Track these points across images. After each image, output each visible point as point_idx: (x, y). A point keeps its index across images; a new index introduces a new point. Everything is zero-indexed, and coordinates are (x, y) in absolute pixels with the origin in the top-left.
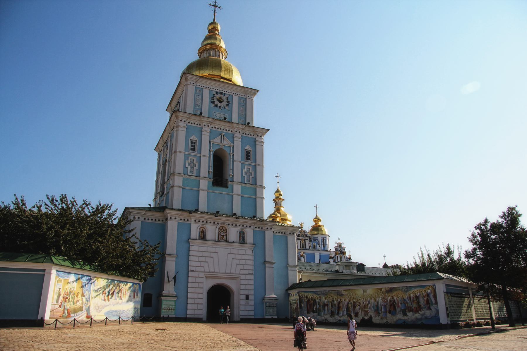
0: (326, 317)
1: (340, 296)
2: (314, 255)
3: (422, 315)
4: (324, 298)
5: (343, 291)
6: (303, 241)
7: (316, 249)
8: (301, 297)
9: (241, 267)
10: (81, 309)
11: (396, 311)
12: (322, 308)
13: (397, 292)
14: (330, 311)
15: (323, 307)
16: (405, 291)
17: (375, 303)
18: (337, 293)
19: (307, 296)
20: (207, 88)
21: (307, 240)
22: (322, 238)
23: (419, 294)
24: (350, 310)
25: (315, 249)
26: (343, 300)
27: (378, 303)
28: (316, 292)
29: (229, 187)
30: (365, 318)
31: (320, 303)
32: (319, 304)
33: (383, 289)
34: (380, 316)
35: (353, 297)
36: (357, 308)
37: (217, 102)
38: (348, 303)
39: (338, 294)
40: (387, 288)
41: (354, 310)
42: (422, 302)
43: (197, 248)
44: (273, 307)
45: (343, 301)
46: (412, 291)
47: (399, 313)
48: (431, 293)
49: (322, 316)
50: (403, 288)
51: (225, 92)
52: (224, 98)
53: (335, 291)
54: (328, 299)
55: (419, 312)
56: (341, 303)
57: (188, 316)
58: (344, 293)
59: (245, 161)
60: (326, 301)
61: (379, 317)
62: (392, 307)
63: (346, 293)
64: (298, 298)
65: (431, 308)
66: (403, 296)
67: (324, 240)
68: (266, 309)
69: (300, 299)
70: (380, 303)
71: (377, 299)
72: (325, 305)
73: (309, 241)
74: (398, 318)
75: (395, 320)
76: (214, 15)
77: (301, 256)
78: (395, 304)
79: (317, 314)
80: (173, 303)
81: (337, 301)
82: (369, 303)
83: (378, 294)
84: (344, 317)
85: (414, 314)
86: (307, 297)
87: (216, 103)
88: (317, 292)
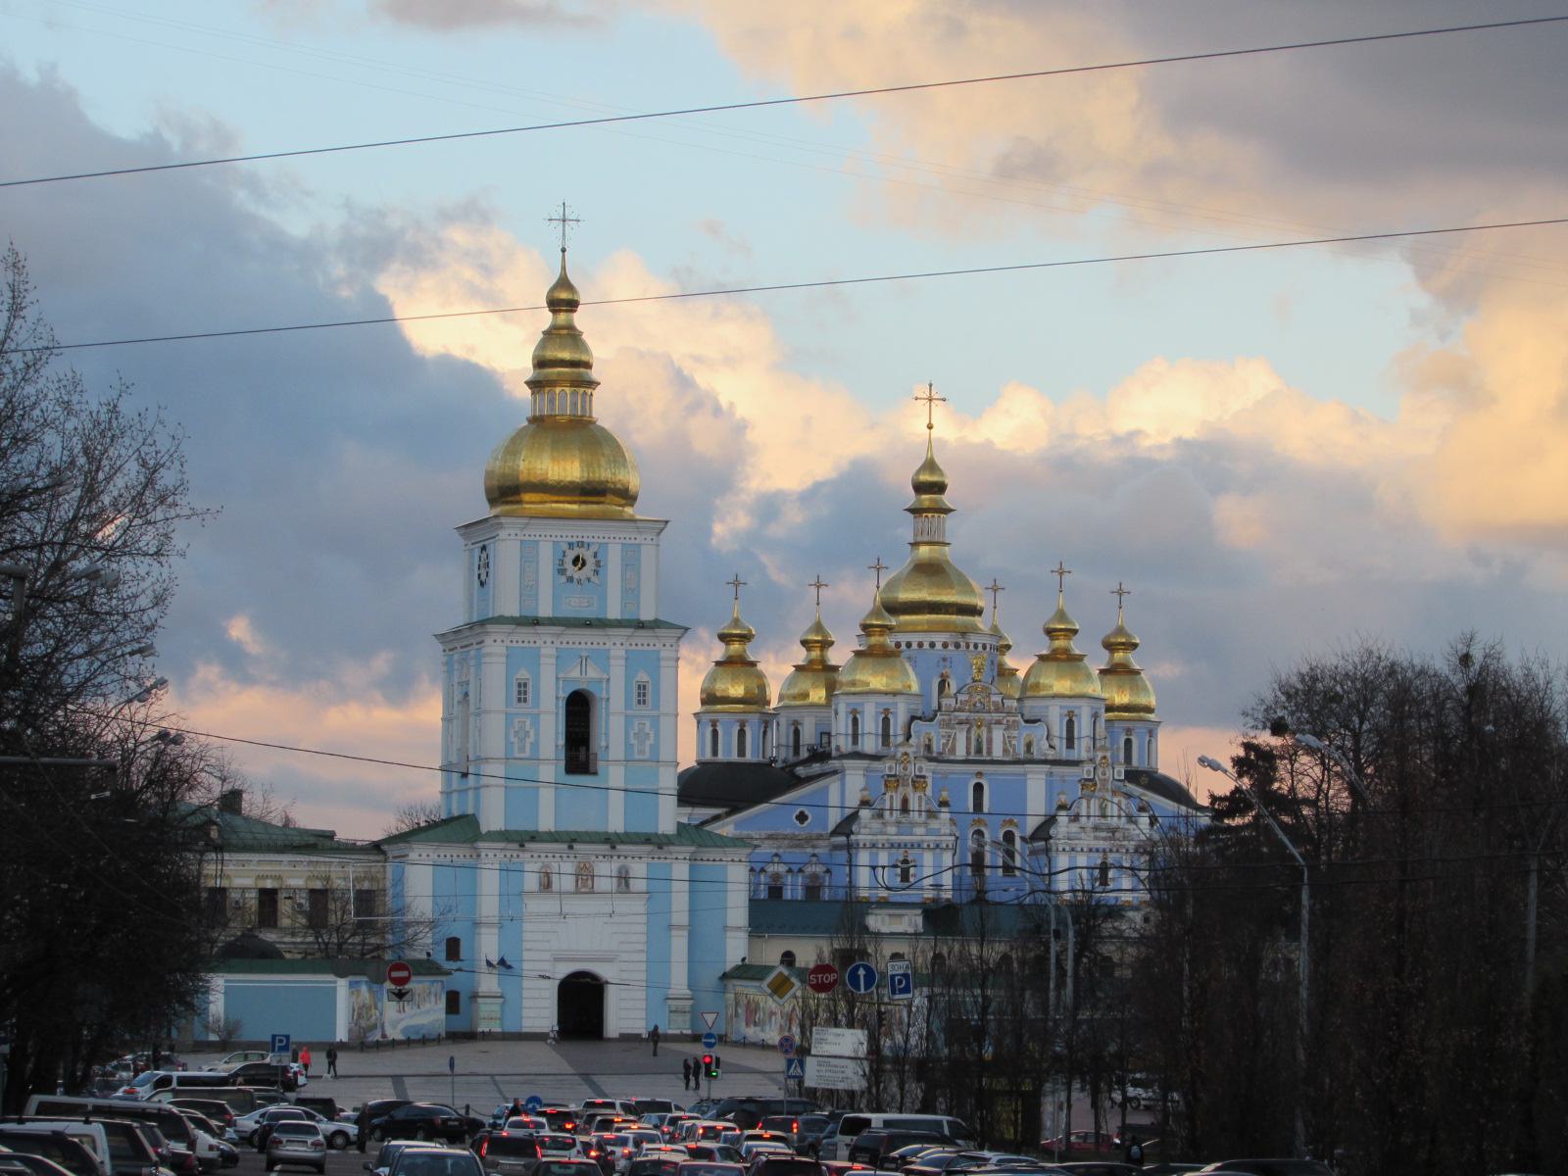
2: (1025, 780)
7: (1036, 756)
10: (375, 1027)
14: (778, 1026)
20: (548, 538)
21: (999, 722)
22: (1065, 712)
25: (1029, 756)
29: (599, 772)
37: (571, 569)
43: (535, 906)
44: (684, 1012)
51: (590, 540)
52: (587, 555)
57: (524, 1030)
59: (632, 709)
67: (1074, 718)
68: (669, 1016)
72: (772, 1013)
73: (1003, 727)
76: (564, 250)
77: (944, 804)
80: (497, 1008)
87: (569, 574)
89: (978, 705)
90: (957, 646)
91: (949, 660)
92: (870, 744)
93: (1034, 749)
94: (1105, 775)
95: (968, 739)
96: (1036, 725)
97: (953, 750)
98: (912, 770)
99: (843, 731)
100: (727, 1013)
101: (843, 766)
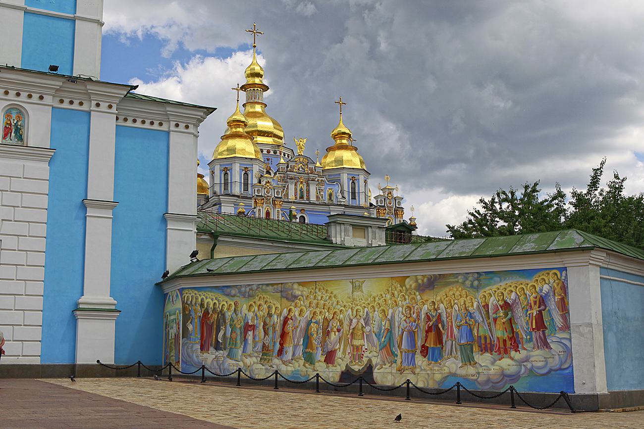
0: (249, 364)
1: (287, 299)
3: (520, 363)
4: (245, 306)
5: (296, 286)
6: (302, 183)
7: (335, 202)
8: (187, 303)
9: (8, 213)
11: (442, 348)
12: (239, 338)
13: (450, 290)
14: (260, 345)
15: (241, 333)
16: (472, 286)
17: (383, 323)
18: (281, 291)
19: (202, 299)
23: (513, 296)
24: (314, 341)
26: (297, 314)
27: (391, 321)
28: (225, 289)
30: (353, 367)
31: (236, 321)
32: (231, 325)
33: (407, 280)
34: (395, 362)
35: (324, 306)
36: (333, 336)
38: (309, 324)
39: (284, 294)
40: (419, 277)
41: (323, 343)
42: (522, 324)
45: (295, 315)
46: (494, 288)
47: (451, 354)
48: (551, 294)
49: (239, 357)
50: (467, 279)
53: (275, 286)
54: (256, 309)
55: (513, 353)
56: (290, 322)
58: (300, 293)
60: (250, 315)
61: (394, 365)
62: (432, 335)
63: (306, 291)
64: (179, 305)
65: (549, 341)
66: (465, 304)
69: (184, 309)
70: (397, 324)
71: (391, 311)
72: (248, 328)
74: (447, 370)
75: (438, 377)
78: (440, 326)
79: (226, 353)
81: (279, 315)
82: (365, 325)
83: (393, 294)
84: (296, 364)
85: (495, 361)
86: (202, 305)
88: (228, 290)
89: (301, 169)
90: (275, 152)
91: (271, 160)
92: (237, 190)
93: (333, 198)
94: (390, 204)
95: (296, 189)
96: (335, 183)
97: (287, 195)
98: (272, 195)
99: (217, 181)
100: (167, 334)
101: (220, 201)
